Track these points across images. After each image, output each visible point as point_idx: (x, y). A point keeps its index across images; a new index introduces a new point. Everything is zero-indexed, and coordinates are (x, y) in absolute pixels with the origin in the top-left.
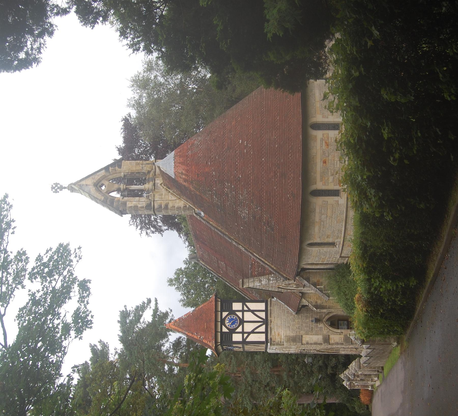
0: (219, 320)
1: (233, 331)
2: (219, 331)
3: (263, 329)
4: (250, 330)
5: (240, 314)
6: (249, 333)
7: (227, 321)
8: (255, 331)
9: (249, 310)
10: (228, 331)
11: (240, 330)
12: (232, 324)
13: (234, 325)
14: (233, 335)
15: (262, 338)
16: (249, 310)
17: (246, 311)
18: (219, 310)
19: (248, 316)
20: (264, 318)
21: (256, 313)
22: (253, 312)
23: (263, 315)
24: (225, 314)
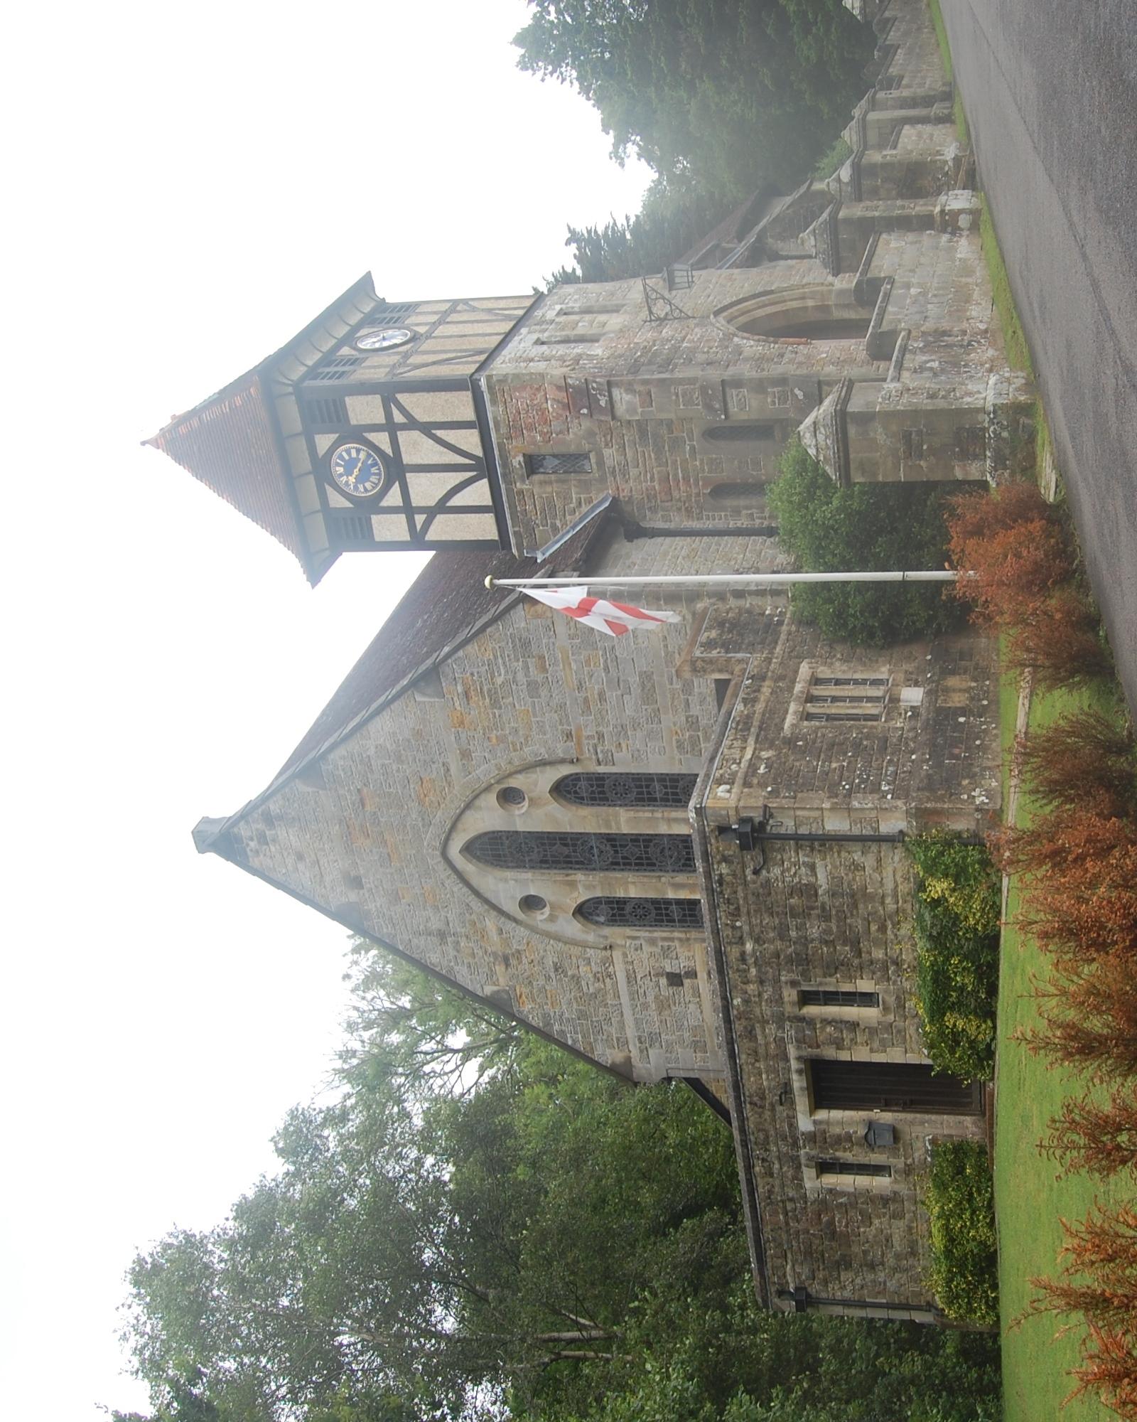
0: (307, 465)
1: (372, 505)
2: (318, 507)
3: (480, 493)
4: (432, 503)
5: (382, 440)
6: (432, 512)
7: (340, 470)
8: (451, 503)
9: (412, 424)
10: (348, 505)
11: (394, 497)
12: (359, 480)
13: (368, 485)
14: (374, 518)
15: (484, 527)
16: (412, 424)
17: (404, 427)
18: (298, 427)
19: (417, 449)
20: (479, 452)
21: (439, 433)
22: (427, 429)
23: (470, 441)
24: (324, 442)
